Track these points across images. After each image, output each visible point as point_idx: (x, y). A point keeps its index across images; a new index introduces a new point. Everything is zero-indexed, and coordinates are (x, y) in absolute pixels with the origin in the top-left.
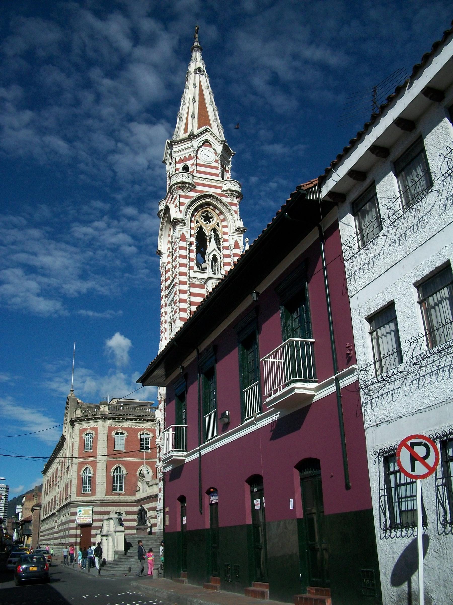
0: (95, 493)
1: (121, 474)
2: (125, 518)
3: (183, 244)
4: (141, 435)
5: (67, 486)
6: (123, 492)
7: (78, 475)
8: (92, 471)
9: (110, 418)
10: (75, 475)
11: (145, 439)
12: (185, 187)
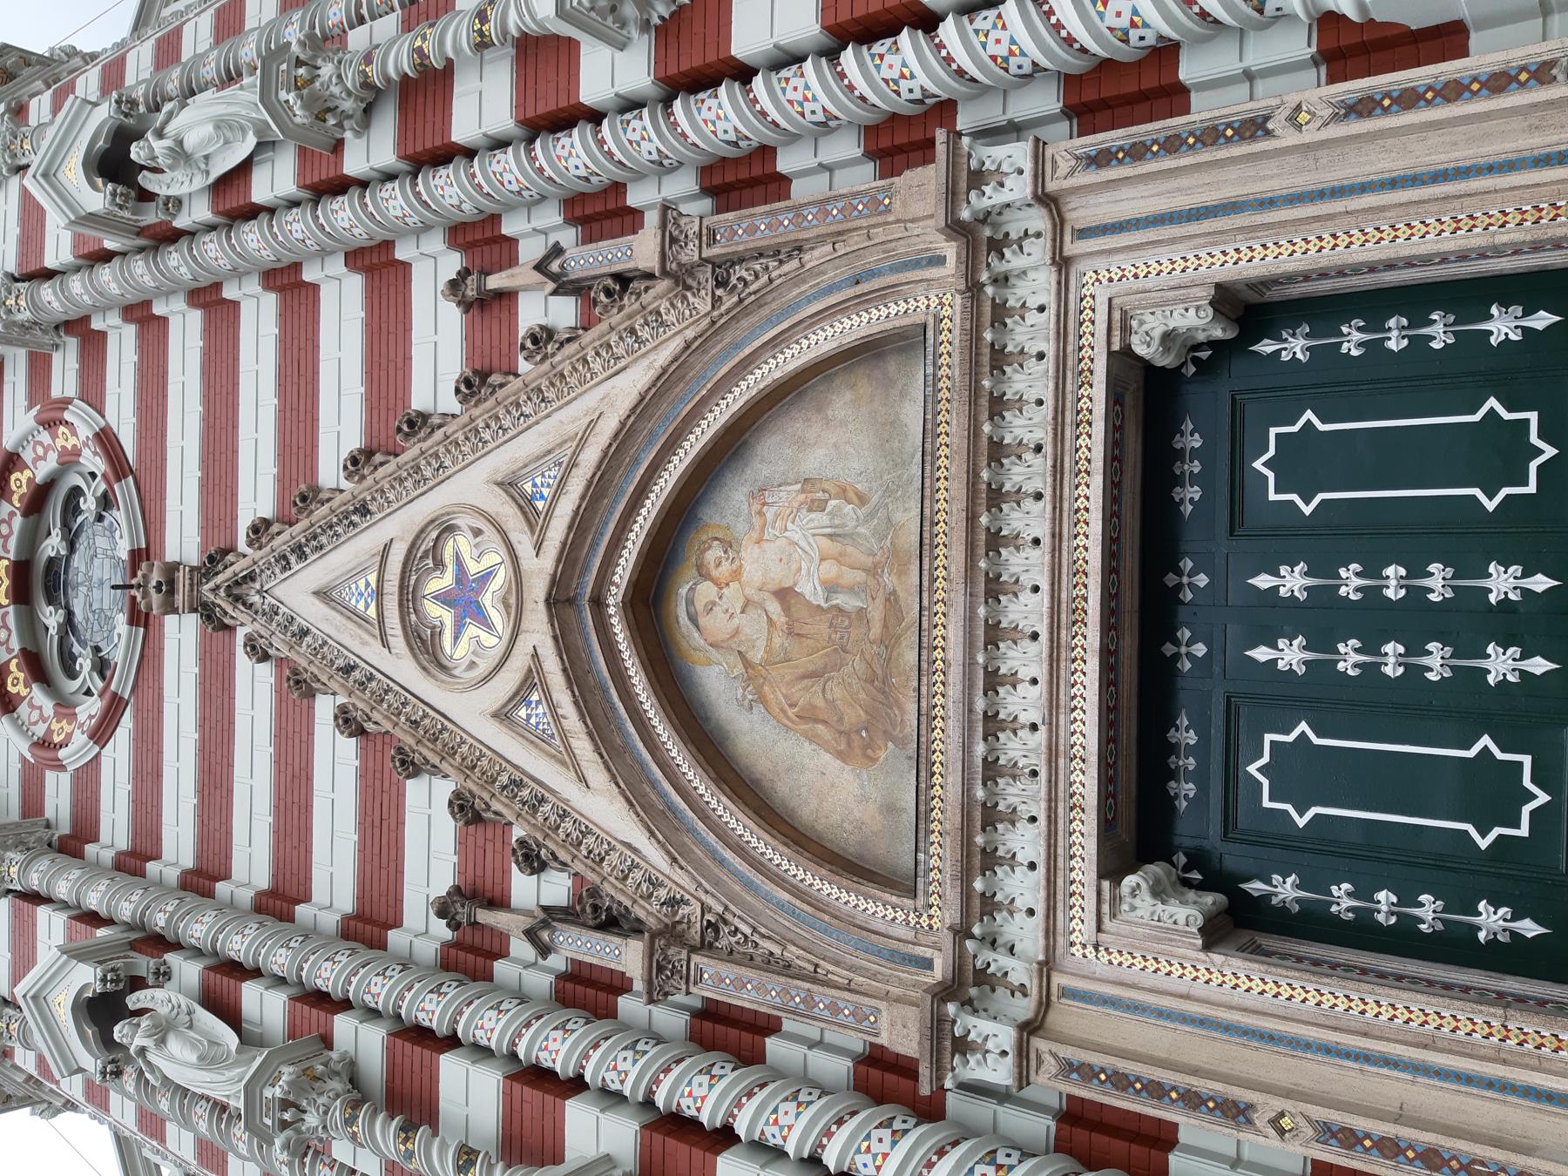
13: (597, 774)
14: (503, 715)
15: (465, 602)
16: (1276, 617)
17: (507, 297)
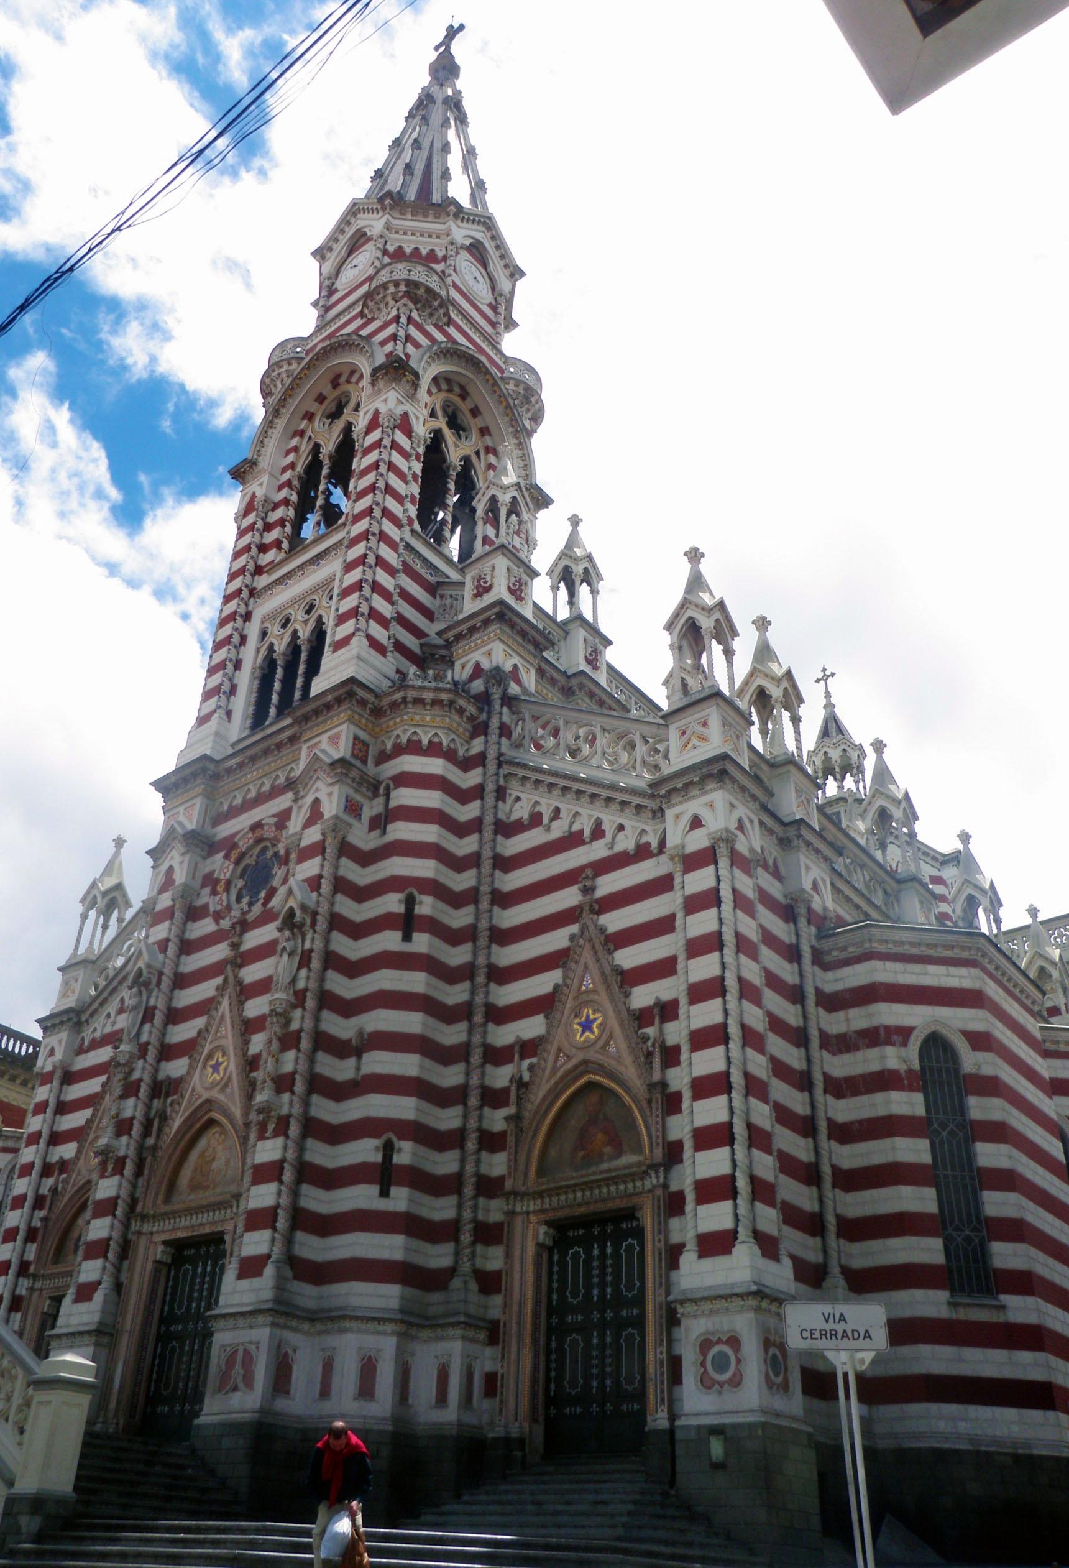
3: (400, 438)
12: (427, 304)
13: (548, 1087)
16: (603, 1249)
17: (652, 1024)
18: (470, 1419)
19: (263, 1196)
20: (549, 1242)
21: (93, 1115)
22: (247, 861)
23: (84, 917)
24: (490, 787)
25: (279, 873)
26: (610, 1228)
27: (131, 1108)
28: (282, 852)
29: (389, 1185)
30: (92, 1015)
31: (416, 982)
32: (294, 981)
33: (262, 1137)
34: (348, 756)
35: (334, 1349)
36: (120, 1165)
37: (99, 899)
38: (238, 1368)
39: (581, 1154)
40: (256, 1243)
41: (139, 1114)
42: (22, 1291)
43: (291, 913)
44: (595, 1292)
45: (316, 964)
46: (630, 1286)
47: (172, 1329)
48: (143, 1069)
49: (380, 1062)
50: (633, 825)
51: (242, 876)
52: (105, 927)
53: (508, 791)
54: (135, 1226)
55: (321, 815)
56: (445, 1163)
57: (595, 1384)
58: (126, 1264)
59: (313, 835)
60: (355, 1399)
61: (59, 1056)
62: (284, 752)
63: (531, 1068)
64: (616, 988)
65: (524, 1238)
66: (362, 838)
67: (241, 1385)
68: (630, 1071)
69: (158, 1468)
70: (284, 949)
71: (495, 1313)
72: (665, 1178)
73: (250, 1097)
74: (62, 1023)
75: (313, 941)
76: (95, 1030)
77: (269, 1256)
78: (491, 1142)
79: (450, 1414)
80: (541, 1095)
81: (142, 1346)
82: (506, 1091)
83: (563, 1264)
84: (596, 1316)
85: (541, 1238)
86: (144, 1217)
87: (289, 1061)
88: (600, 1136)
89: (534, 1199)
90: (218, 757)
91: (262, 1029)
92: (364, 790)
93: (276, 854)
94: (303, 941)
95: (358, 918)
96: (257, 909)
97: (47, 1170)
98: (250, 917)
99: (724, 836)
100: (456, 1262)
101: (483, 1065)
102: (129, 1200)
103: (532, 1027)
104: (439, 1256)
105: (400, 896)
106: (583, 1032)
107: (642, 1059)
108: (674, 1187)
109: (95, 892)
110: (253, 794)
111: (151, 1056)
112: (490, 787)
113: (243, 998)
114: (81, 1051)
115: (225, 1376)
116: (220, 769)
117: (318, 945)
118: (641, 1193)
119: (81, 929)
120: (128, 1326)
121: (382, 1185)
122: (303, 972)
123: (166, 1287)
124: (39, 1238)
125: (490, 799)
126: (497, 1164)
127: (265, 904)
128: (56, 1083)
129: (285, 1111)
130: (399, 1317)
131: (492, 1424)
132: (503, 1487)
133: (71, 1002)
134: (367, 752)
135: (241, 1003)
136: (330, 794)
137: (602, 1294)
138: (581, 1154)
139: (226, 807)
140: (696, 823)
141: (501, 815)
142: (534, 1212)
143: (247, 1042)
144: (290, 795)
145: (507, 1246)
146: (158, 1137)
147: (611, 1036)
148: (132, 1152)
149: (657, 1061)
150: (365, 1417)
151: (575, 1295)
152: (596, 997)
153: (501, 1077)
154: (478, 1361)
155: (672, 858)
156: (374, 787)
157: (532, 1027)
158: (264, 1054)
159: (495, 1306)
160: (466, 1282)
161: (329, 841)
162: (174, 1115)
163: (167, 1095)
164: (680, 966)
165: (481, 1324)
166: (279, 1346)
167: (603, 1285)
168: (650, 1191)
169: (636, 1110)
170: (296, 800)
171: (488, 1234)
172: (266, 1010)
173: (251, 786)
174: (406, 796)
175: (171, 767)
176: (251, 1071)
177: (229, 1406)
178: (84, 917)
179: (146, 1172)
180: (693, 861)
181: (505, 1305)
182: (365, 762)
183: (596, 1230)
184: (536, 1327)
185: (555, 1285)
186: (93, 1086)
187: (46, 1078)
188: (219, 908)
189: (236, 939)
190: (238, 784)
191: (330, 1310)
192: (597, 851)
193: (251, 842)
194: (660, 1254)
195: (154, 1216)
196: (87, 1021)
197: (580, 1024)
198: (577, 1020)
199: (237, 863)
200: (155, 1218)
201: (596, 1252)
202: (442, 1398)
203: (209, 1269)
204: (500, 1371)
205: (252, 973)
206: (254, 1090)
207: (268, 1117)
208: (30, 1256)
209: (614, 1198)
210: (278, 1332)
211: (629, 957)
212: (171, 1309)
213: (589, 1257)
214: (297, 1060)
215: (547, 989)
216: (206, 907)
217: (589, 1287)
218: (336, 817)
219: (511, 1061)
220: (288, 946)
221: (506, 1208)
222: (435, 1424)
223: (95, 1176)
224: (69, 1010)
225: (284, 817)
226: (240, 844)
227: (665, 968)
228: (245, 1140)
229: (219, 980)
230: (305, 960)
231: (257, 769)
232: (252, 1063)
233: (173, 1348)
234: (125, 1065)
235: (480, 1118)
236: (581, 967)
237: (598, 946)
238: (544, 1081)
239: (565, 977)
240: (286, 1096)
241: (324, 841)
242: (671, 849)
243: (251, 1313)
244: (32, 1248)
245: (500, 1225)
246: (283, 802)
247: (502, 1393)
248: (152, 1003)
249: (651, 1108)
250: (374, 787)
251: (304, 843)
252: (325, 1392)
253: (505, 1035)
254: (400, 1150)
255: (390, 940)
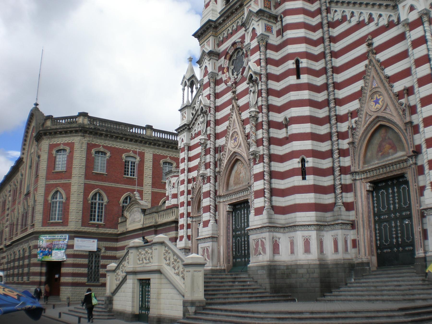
0: (68, 222)
1: (101, 201)
2: (104, 254)
4: (126, 157)
5: (25, 216)
6: (102, 223)
7: (46, 200)
8: (64, 196)
9: (91, 133)
10: (40, 199)
11: (130, 162)
13: (364, 128)
14: (367, 113)
15: (377, 102)
16: (393, 190)
17: (403, 97)
18: (348, 257)
19: (259, 185)
20: (371, 189)
21: (200, 160)
22: (234, 58)
23: (184, 90)
24: (324, 8)
25: (245, 60)
26: (395, 182)
27: (209, 158)
28: (245, 52)
29: (305, 175)
30: (193, 125)
31: (305, 95)
32: (257, 103)
33: (255, 164)
34: (263, 8)
35: (293, 237)
36: (209, 179)
37: (187, 82)
38: (260, 247)
39: (380, 154)
40: (258, 203)
41: (212, 160)
42: (189, 222)
43: (251, 76)
44: (392, 206)
45: (264, 95)
46: (405, 203)
47: (237, 233)
48: (210, 144)
49: (295, 129)
50: (385, 14)
51: (232, 65)
52: (192, 92)
53: (331, 9)
54: (218, 200)
55: (257, 34)
56: (326, 164)
57: (395, 240)
58: (217, 213)
59: (254, 43)
60: (303, 254)
61: (185, 141)
62: (239, 11)
63: (356, 122)
64: (387, 84)
65: (361, 189)
66: (274, 40)
67: (262, 253)
68: (396, 119)
69: (236, 283)
70: (251, 90)
71: (352, 218)
72: (416, 160)
73: (249, 150)
74: (184, 129)
75: (262, 86)
76: (195, 130)
77: (264, 207)
78: (343, 153)
79: (340, 256)
80: (361, 132)
81: (228, 240)
82: (347, 132)
83: (378, 197)
84: (393, 215)
85: (368, 188)
86: (220, 196)
87: (260, 134)
88: (387, 146)
89: (363, 173)
90: (214, 19)
91: (248, 123)
92: (272, 20)
93: (243, 53)
94: (258, 86)
95: (278, 73)
96: (240, 76)
97: (189, 181)
98: (237, 80)
99: (425, 12)
100: (336, 201)
101: (336, 123)
102: (214, 191)
103: (354, 105)
104: (328, 199)
105: (293, 61)
106: (376, 104)
107: (401, 113)
108: (419, 163)
109: (185, 80)
110: (230, 31)
111: (212, 139)
112: (324, 8)
113: (240, 112)
114: (192, 138)
115: (256, 250)
116: (217, 23)
117: (264, 87)
118: (406, 167)
119: (184, 94)
120: (222, 234)
121: (302, 175)
122: (260, 99)
123: (233, 220)
124: (191, 204)
125: (324, 14)
126: (346, 162)
127: (242, 74)
128: (186, 151)
129: (261, 153)
130: (316, 223)
131: (356, 257)
132: (362, 281)
133: (185, 122)
134: (270, 4)
135: (240, 114)
136: (258, 25)
137: (394, 207)
138: (380, 154)
139: (221, 39)
140: (412, 8)
141: (330, 19)
142: (364, 178)
143: (245, 129)
144: (244, 29)
145: (355, 193)
146: (220, 167)
147: (387, 105)
148: (212, 174)
149: (407, 112)
150: (308, 260)
151: (384, 208)
152: (379, 90)
153: (344, 127)
154: (348, 236)
155: (404, 26)
156: (275, 18)
157: (354, 105)
158: (251, 133)
159: (351, 215)
160: (340, 208)
161: (261, 44)
162: (224, 159)
163: (220, 152)
164: (413, 71)
165: (348, 222)
166: (273, 238)
167: (394, 203)
168: (410, 166)
169: (401, 134)
170: (246, 31)
171: (346, 188)
172: (248, 115)
173: (229, 28)
174: (289, 19)
175: (199, 27)
176: (248, 139)
177: (258, 260)
178: (184, 90)
179: (218, 180)
180: (413, 25)
181: (357, 214)
182: (270, 9)
183: (390, 183)
184: (369, 221)
185: (376, 205)
186: (198, 150)
187: (183, 150)
188: (226, 79)
189: (234, 90)
190: (224, 28)
191: (290, 223)
192: (372, 27)
193: (233, 50)
194: (416, 191)
195: (223, 196)
196: (192, 127)
197: (374, 101)
198: (372, 100)
199: (230, 60)
200: (224, 196)
201: (390, 191)
202: (336, 250)
203: (246, 212)
204: (357, 239)
205: (242, 102)
206: (250, 146)
207: (256, 156)
208: (190, 211)
209: (395, 170)
210: (272, 233)
211: (390, 71)
212: (236, 226)
213: (388, 194)
214: (263, 133)
215: (359, 89)
216: (221, 78)
217: (389, 204)
218: (262, 34)
219: (347, 120)
220: (253, 89)
221: (352, 178)
222: (335, 260)
223: (201, 185)
224: (185, 125)
225: (243, 37)
226: (229, 52)
227: (407, 73)
228: (250, 164)
229: (231, 107)
230: (260, 94)
231: (230, 21)
232: (248, 136)
233: (239, 240)
234: (203, 144)
235: (338, 144)
236: (371, 78)
237: (378, 68)
238: (362, 127)
239: (365, 83)
240: (261, 147)
241: (259, 45)
242: (403, 21)
243: (261, 228)
244: (190, 208)
245: (351, 185)
246: (242, 32)
247: (359, 247)
248: (209, 119)
249: (407, 132)
250: (275, 18)
251: (251, 47)
252: (292, 252)
253: (343, 110)
254: (307, 162)
255: (292, 80)
